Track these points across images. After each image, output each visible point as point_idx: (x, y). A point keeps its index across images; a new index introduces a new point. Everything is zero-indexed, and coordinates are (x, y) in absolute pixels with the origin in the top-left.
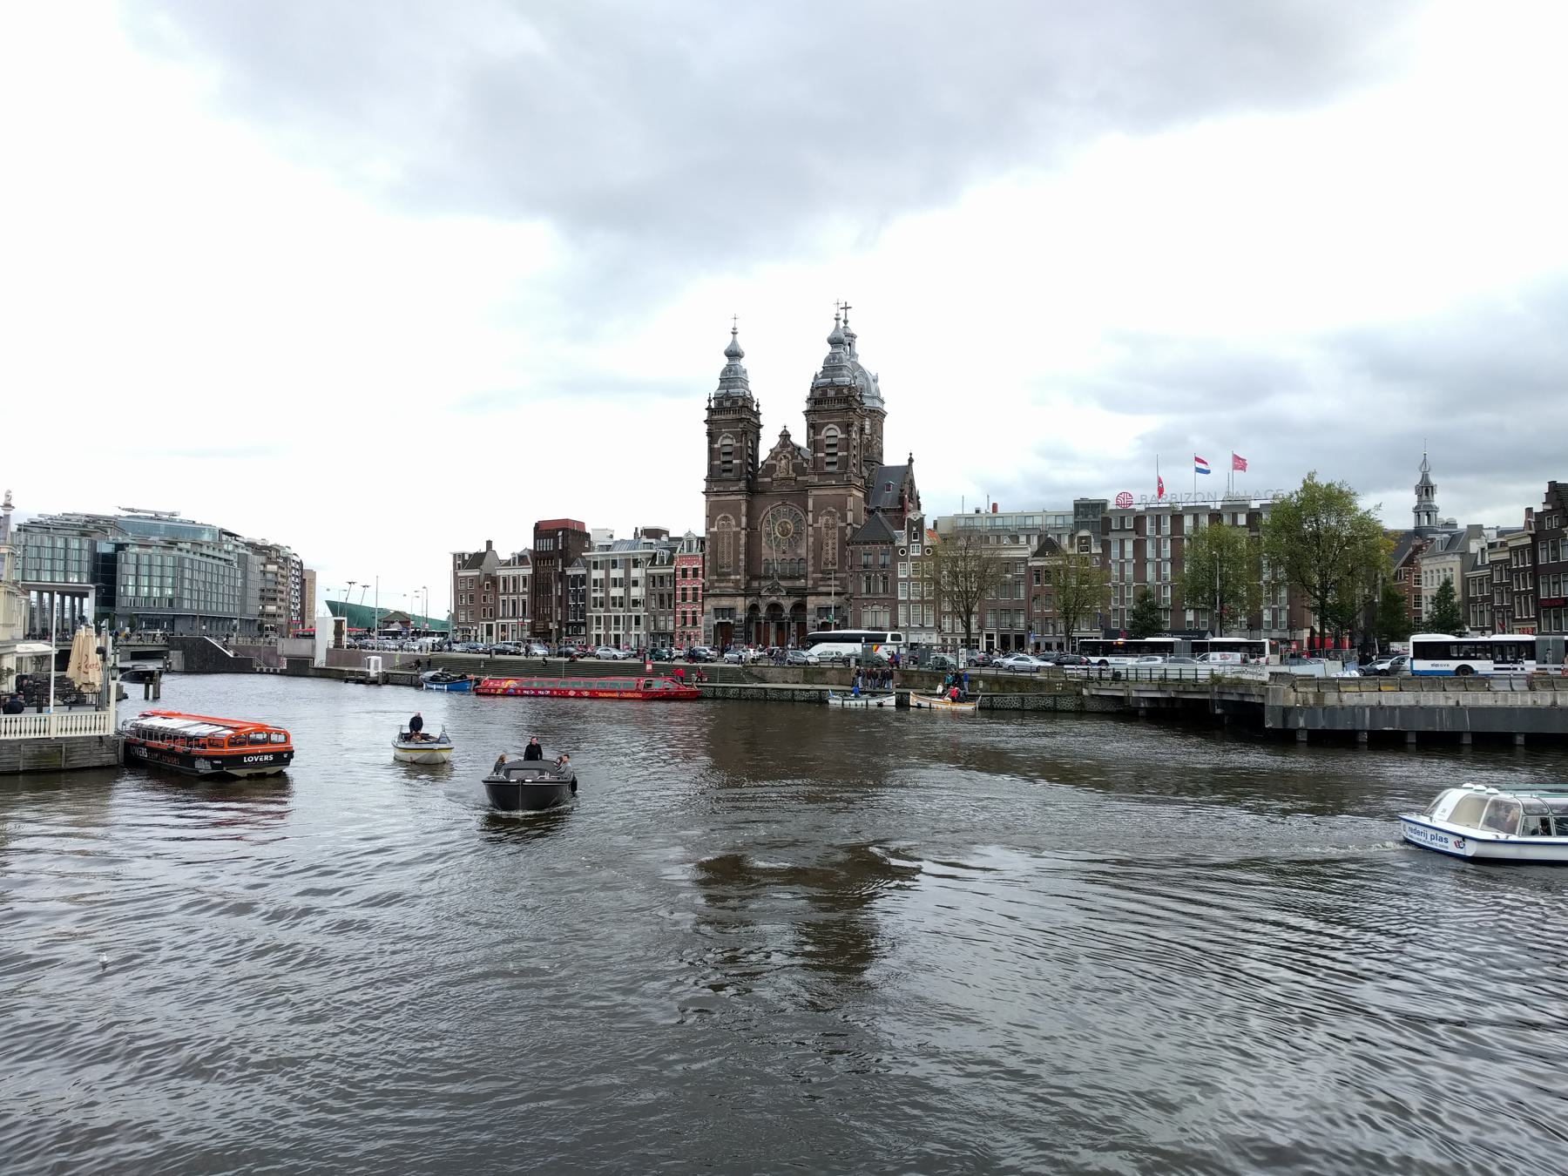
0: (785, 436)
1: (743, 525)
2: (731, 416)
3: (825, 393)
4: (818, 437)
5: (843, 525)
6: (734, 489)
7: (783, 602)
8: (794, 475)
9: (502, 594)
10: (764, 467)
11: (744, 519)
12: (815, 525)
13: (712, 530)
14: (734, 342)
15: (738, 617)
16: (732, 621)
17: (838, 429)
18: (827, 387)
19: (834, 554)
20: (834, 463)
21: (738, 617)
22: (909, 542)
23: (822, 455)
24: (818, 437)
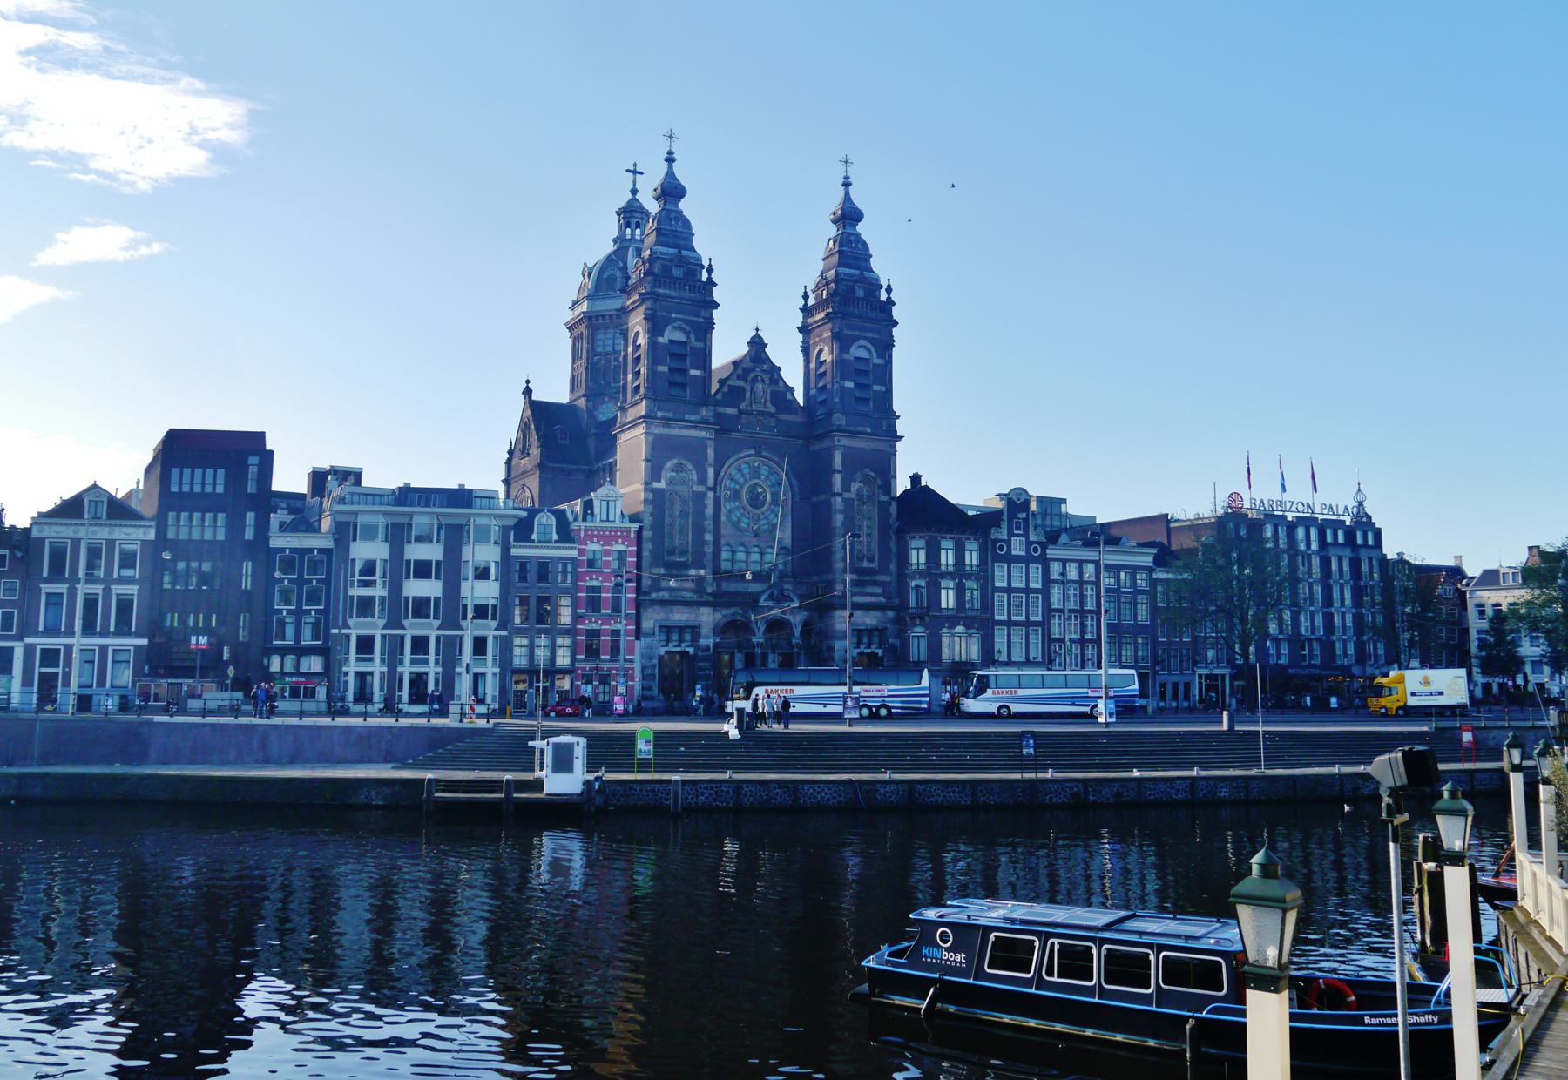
0: (757, 344)
1: (711, 482)
2: (688, 294)
3: (852, 290)
4: (846, 357)
5: (884, 498)
6: (693, 418)
7: (791, 618)
8: (772, 410)
9: (48, 581)
10: (725, 389)
11: (711, 472)
12: (846, 495)
13: (656, 485)
14: (670, 175)
15: (703, 642)
16: (691, 650)
17: (873, 350)
18: (855, 281)
19: (869, 543)
20: (866, 401)
21: (703, 642)
22: (1010, 534)
23: (850, 384)
24: (846, 357)
